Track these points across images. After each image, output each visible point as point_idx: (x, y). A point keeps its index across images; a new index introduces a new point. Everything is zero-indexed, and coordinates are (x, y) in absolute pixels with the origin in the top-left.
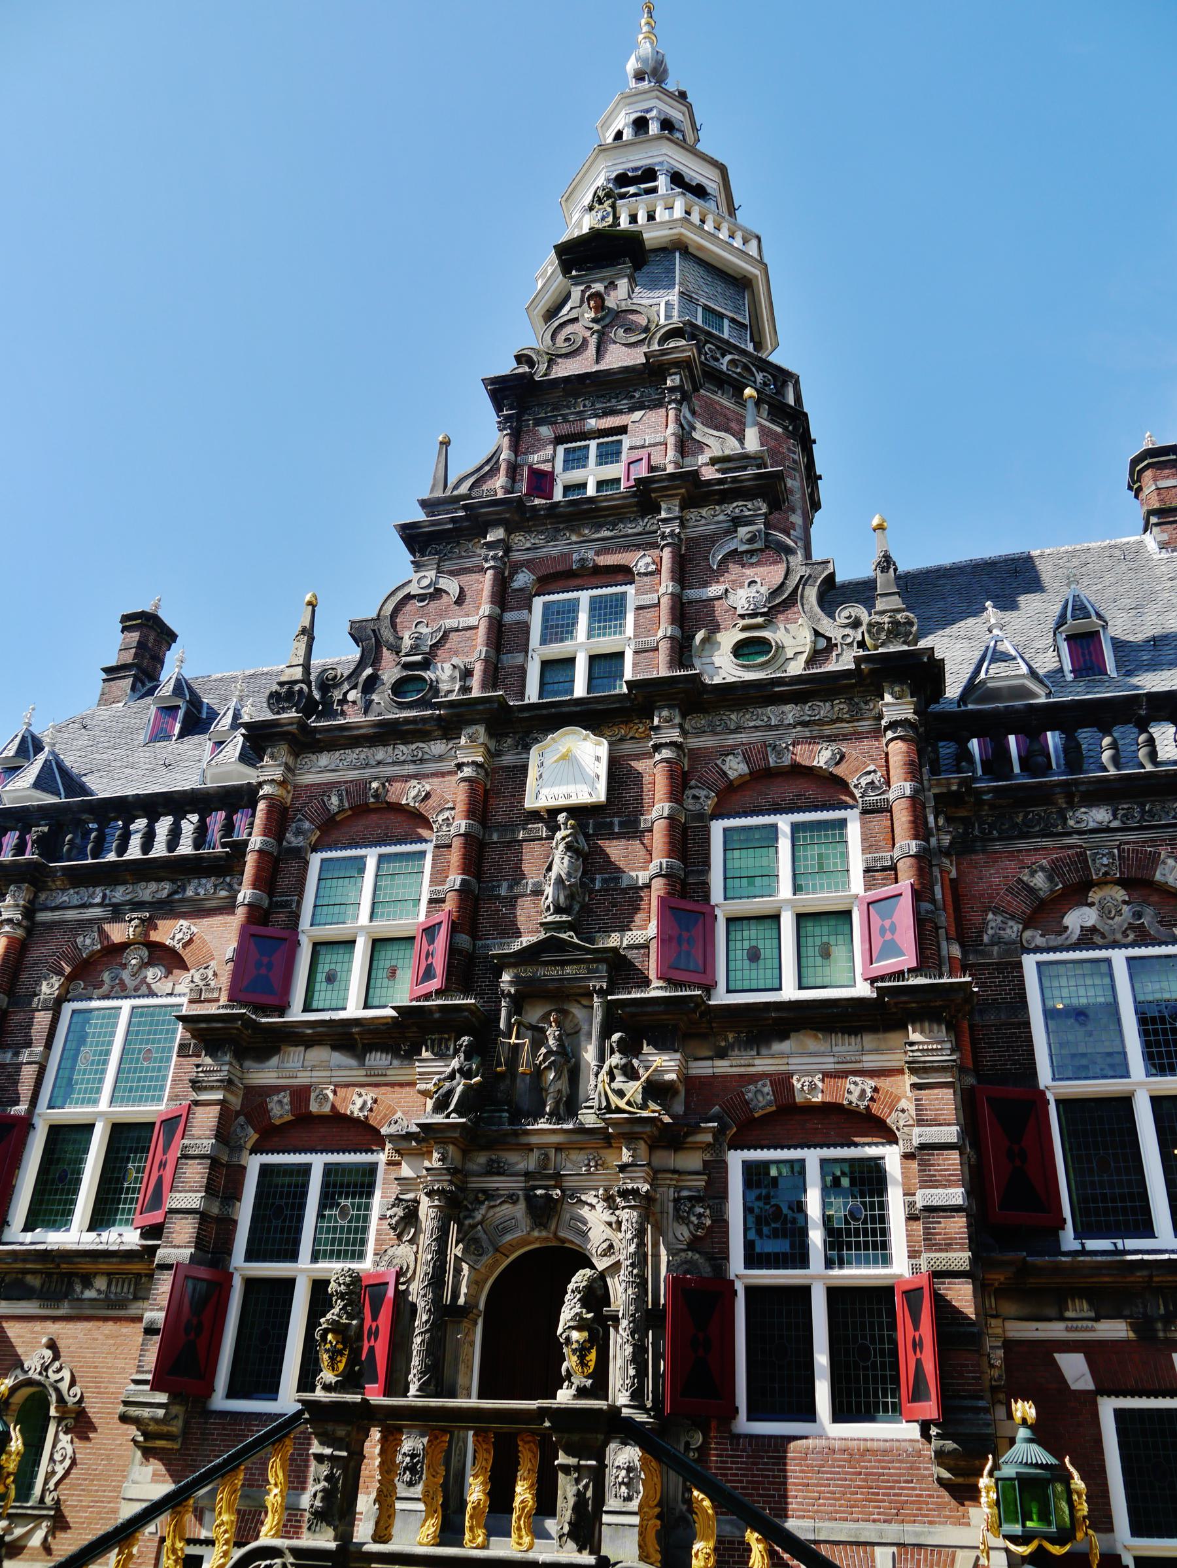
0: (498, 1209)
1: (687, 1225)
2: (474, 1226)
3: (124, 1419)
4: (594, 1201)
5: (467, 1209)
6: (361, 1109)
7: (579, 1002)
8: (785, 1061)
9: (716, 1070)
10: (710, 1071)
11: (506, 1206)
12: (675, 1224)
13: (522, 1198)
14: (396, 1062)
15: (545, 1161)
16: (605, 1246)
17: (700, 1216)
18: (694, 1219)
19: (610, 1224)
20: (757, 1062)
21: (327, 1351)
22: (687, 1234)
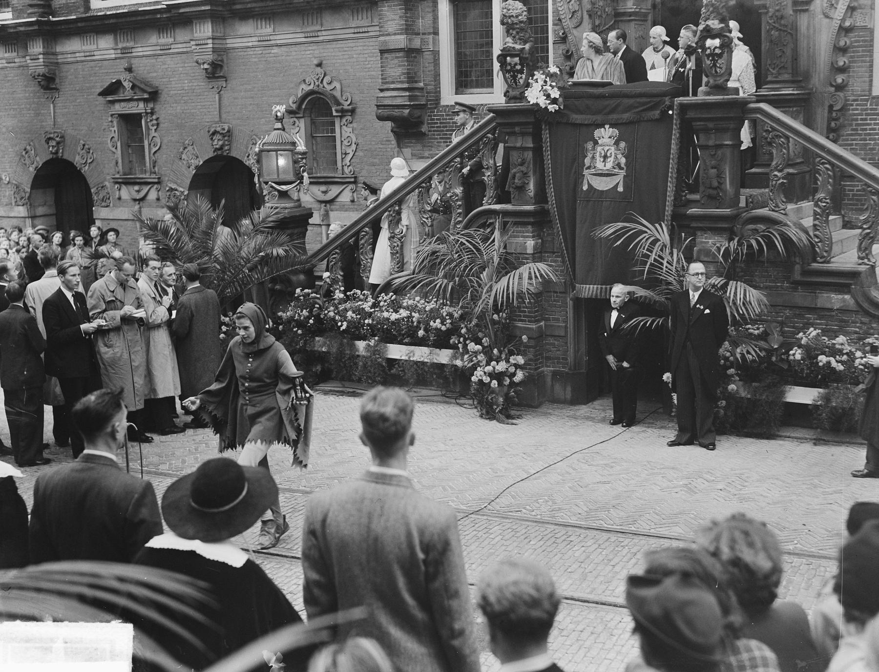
3: (381, 118)
21: (508, 71)
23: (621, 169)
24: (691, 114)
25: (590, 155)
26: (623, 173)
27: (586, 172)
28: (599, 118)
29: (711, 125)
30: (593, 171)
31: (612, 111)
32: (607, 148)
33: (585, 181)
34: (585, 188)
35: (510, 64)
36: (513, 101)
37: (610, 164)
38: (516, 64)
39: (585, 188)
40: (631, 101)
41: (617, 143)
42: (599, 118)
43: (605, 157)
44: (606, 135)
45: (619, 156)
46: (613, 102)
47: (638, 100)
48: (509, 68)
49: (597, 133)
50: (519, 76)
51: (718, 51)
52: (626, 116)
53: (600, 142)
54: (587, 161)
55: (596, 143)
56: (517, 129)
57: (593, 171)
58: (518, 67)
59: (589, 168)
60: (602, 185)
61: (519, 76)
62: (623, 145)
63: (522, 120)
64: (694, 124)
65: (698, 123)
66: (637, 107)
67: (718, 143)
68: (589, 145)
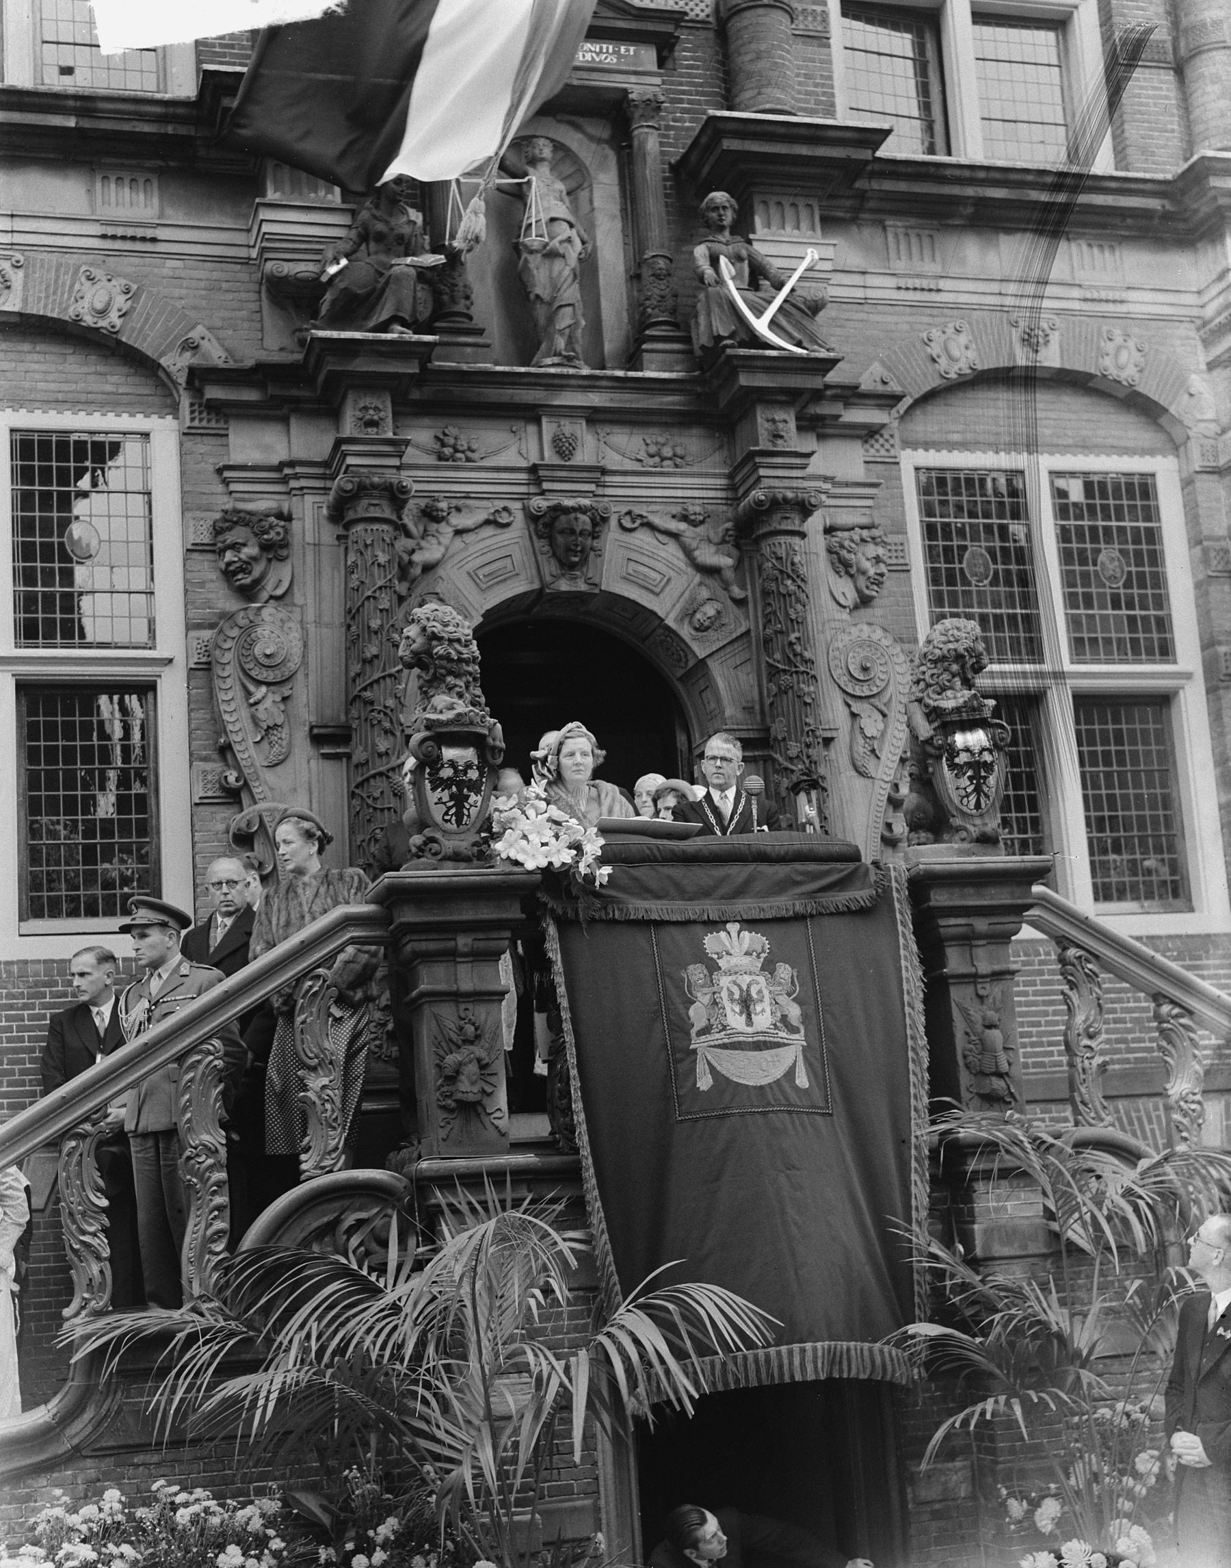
0: (469, 538)
1: (852, 576)
2: (428, 568)
4: (674, 526)
5: (408, 535)
6: (103, 313)
7: (577, 127)
8: (995, 287)
9: (870, 293)
10: (859, 293)
11: (489, 531)
12: (832, 577)
13: (519, 519)
14: (176, 216)
15: (564, 447)
16: (710, 610)
17: (878, 560)
18: (867, 565)
19: (710, 571)
20: (942, 284)
22: (851, 597)
23: (793, 1030)
24: (940, 898)
25: (703, 998)
26: (799, 1039)
27: (697, 1043)
28: (711, 909)
29: (981, 924)
30: (717, 1037)
31: (740, 892)
32: (748, 978)
33: (701, 1067)
34: (705, 1083)
35: (453, 764)
36: (450, 864)
37: (764, 1019)
38: (469, 766)
39: (705, 1083)
40: (782, 870)
41: (769, 967)
42: (711, 909)
43: (746, 1004)
44: (736, 948)
45: (783, 999)
46: (739, 872)
47: (799, 866)
48: (447, 773)
49: (712, 942)
50: (473, 798)
51: (987, 757)
52: (783, 904)
53: (721, 963)
54: (697, 1014)
55: (712, 967)
56: (463, 942)
57: (717, 1037)
58: (473, 774)
59: (705, 1031)
60: (755, 1071)
61: (473, 798)
62: (784, 971)
63: (486, 913)
64: (942, 922)
65: (953, 921)
66: (798, 883)
67: (997, 968)
68: (696, 972)
